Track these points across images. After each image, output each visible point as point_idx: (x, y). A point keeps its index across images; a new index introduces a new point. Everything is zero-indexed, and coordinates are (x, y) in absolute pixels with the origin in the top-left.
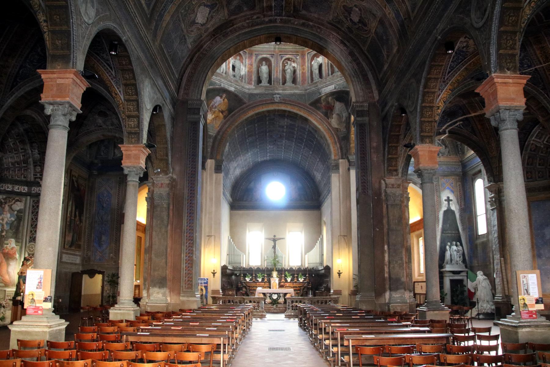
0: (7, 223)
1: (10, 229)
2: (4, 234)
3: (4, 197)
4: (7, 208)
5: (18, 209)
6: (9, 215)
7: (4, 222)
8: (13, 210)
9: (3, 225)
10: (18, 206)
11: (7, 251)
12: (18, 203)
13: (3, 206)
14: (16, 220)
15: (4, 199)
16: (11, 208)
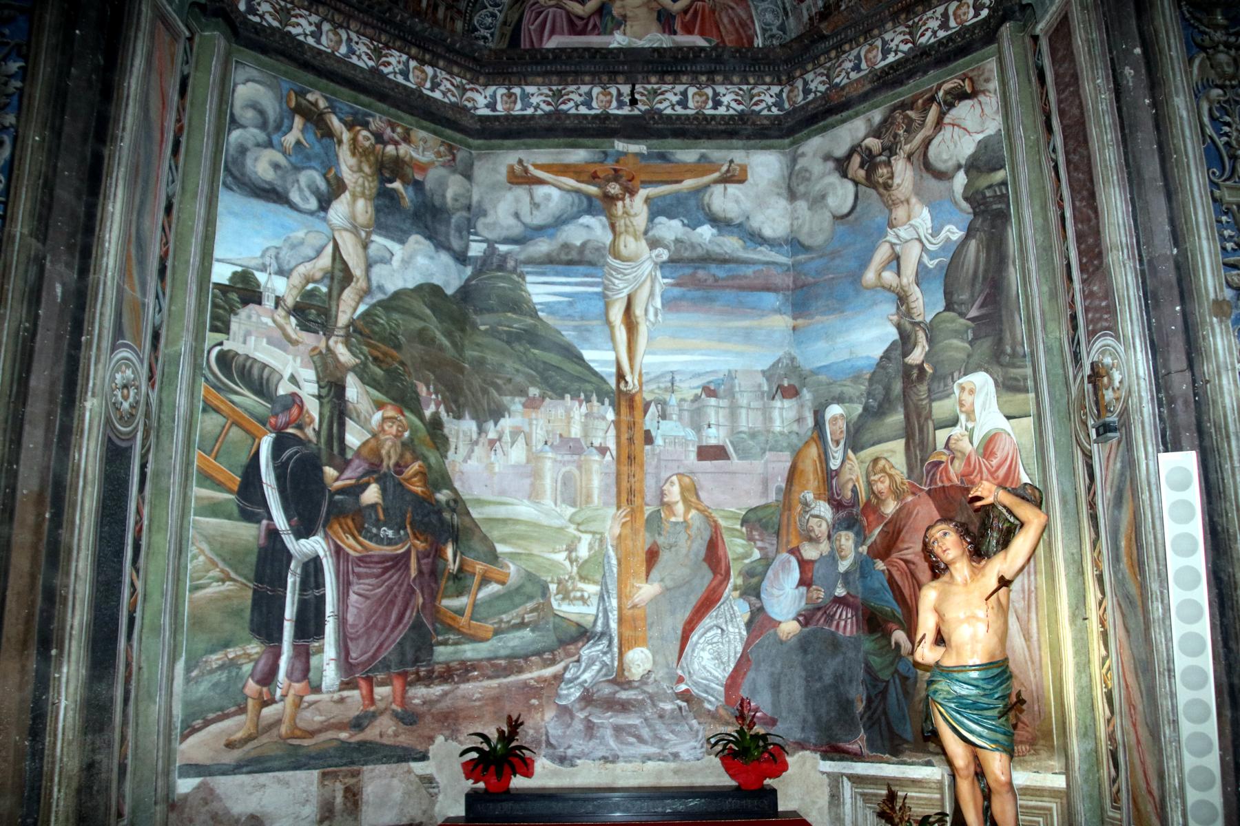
0: (922, 275)
1: (949, 307)
2: (917, 356)
3: (877, 116)
4: (903, 173)
5: (967, 147)
6: (923, 218)
7: (909, 268)
8: (940, 175)
9: (902, 299)
10: (969, 128)
11: (955, 471)
12: (964, 111)
13: (882, 171)
14: (968, 236)
15: (877, 133)
16: (927, 166)
